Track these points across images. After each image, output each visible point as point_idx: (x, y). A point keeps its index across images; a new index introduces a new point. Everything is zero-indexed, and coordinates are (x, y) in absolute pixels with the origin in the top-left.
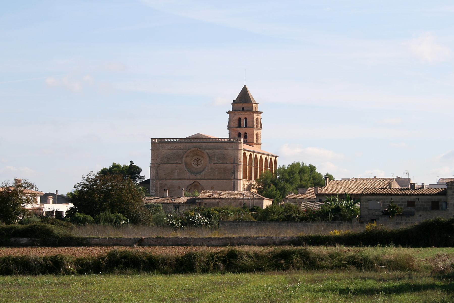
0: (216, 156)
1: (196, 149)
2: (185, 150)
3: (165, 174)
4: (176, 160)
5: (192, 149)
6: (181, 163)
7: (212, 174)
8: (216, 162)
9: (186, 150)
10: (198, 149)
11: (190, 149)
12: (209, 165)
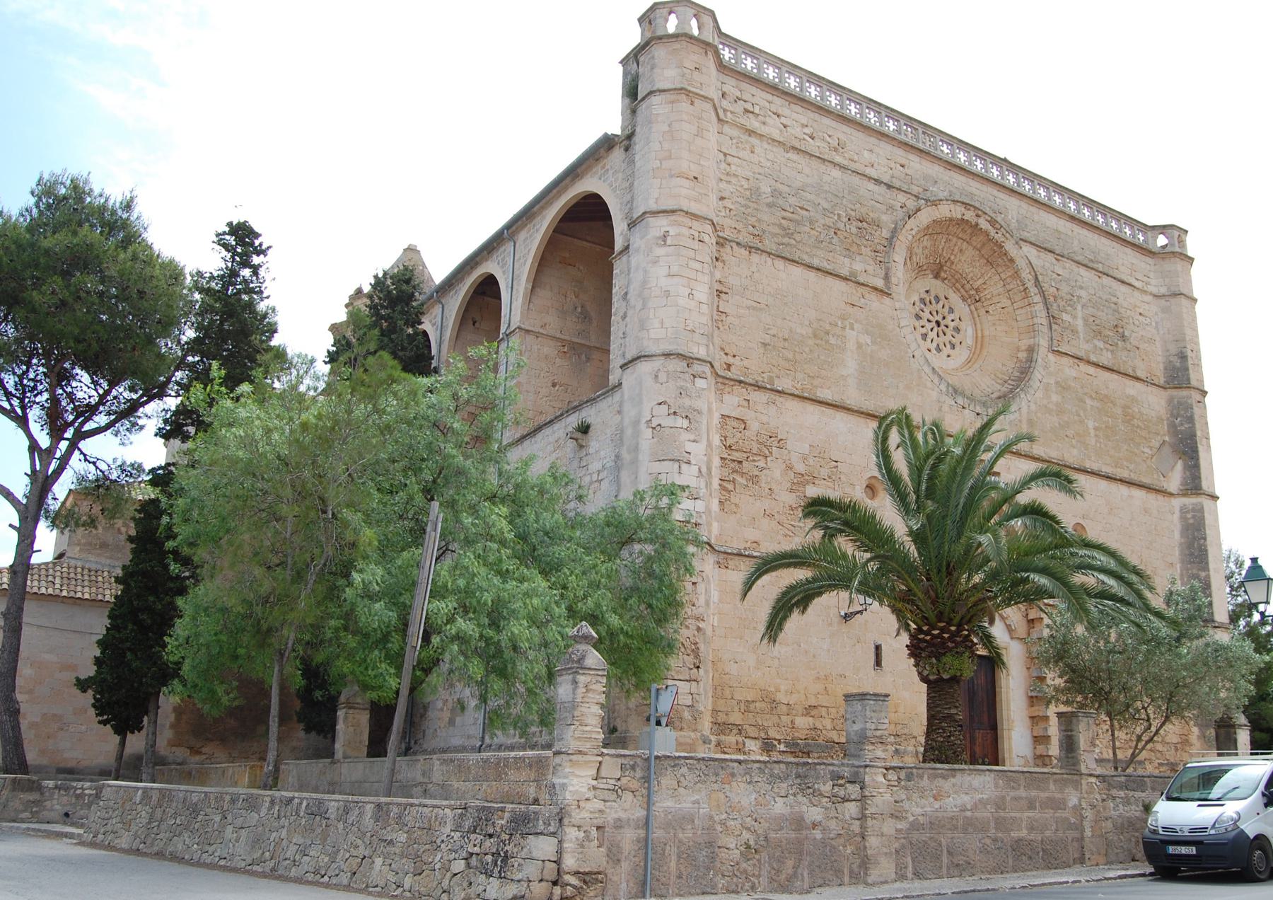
0: (1079, 308)
1: (970, 215)
2: (902, 198)
3: (765, 345)
4: (848, 252)
5: (945, 211)
6: (880, 283)
7: (1070, 432)
8: (1082, 348)
9: (911, 204)
10: (983, 224)
11: (935, 203)
12: (1051, 356)
